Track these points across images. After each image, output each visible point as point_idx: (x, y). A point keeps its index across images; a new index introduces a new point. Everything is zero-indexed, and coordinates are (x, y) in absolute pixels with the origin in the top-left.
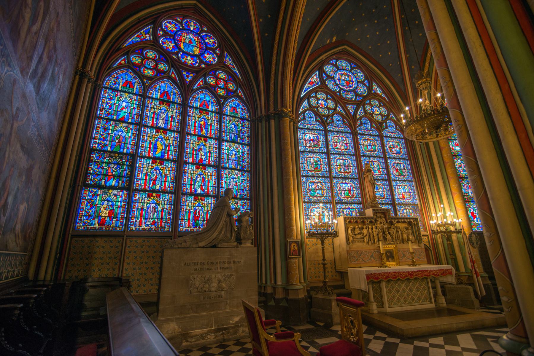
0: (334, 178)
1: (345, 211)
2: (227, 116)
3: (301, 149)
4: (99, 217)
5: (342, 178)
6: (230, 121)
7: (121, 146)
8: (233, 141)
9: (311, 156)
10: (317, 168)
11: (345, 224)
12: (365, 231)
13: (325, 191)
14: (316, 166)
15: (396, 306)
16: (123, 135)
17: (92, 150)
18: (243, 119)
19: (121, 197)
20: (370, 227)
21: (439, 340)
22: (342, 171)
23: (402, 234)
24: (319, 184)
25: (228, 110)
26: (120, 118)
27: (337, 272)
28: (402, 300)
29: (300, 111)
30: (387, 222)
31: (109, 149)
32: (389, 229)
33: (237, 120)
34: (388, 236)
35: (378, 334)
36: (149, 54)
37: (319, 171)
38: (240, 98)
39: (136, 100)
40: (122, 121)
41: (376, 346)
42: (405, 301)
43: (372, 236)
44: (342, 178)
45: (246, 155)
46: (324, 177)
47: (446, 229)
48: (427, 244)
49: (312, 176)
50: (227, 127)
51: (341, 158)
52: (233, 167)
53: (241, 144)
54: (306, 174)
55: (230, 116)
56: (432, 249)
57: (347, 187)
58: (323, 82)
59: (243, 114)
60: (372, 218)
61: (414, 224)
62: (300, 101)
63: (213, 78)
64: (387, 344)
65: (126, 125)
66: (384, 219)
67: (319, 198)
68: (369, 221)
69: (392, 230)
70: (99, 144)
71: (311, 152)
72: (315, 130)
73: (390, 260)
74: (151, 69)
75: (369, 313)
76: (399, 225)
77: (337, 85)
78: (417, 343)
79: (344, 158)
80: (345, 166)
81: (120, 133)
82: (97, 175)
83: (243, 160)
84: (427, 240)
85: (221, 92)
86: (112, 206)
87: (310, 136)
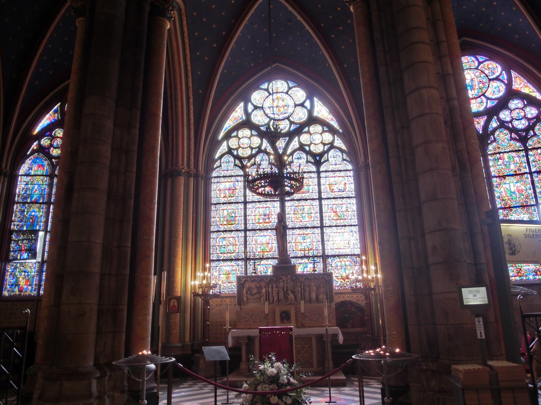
0: (250, 230)
1: (259, 267)
3: (214, 201)
4: (18, 285)
5: (260, 230)
7: (34, 225)
9: (225, 208)
12: (264, 290)
13: (237, 247)
16: (36, 215)
17: (12, 232)
19: (35, 268)
22: (261, 221)
24: (231, 239)
26: (33, 200)
29: (217, 156)
31: (25, 229)
34: (291, 296)
36: (57, 133)
37: (232, 224)
39: (46, 181)
40: (36, 202)
43: (270, 295)
44: (260, 230)
47: (366, 286)
49: (223, 231)
51: (261, 206)
54: (217, 229)
57: (264, 240)
58: (248, 115)
62: (219, 143)
65: (38, 205)
67: (229, 255)
70: (18, 225)
71: (226, 203)
72: (232, 176)
73: (285, 321)
74: (58, 148)
77: (267, 115)
79: (265, 206)
80: (265, 215)
81: (33, 214)
82: (16, 251)
86: (28, 276)
87: (225, 184)
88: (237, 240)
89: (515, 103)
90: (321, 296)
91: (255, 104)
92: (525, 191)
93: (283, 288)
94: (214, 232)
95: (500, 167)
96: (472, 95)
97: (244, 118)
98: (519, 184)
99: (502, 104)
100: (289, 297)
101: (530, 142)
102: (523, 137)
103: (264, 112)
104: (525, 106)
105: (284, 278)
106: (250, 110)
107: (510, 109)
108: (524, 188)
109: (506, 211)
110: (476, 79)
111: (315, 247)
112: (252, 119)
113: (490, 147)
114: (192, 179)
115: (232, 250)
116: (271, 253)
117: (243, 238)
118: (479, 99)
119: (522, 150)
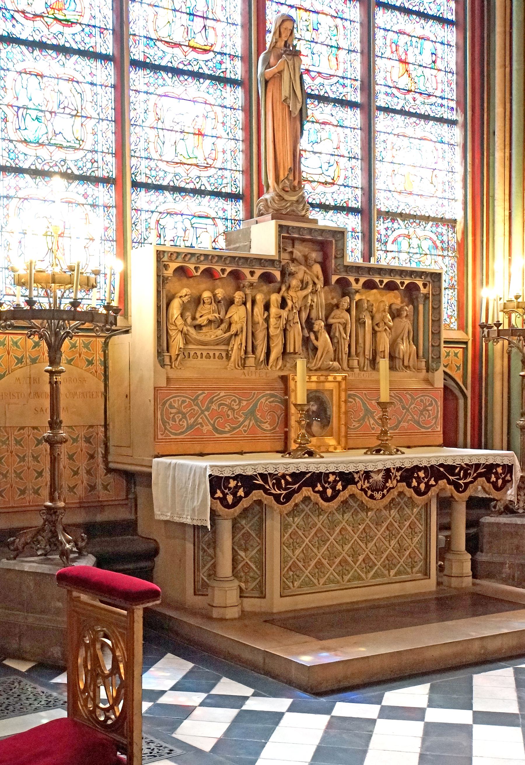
0: (136, 64)
11: (161, 281)
12: (238, 314)
13: (90, 124)
15: (305, 590)
20: (259, 297)
21: (415, 695)
23: (374, 333)
27: (109, 471)
28: (331, 571)
30: (327, 282)
32: (331, 308)
35: (227, 687)
41: (205, 727)
42: (342, 575)
43: (261, 335)
48: (458, 376)
56: (468, 393)
60: (271, 262)
61: (426, 297)
64: (244, 716)
66: (317, 268)
68: (258, 272)
69: (340, 317)
75: (209, 618)
76: (373, 295)
78: (343, 709)
84: (460, 362)
88: (88, 96)
90: (403, 347)
93: (299, 312)
100: (319, 344)
105: (300, 275)
111: (343, 174)
116: (211, 172)
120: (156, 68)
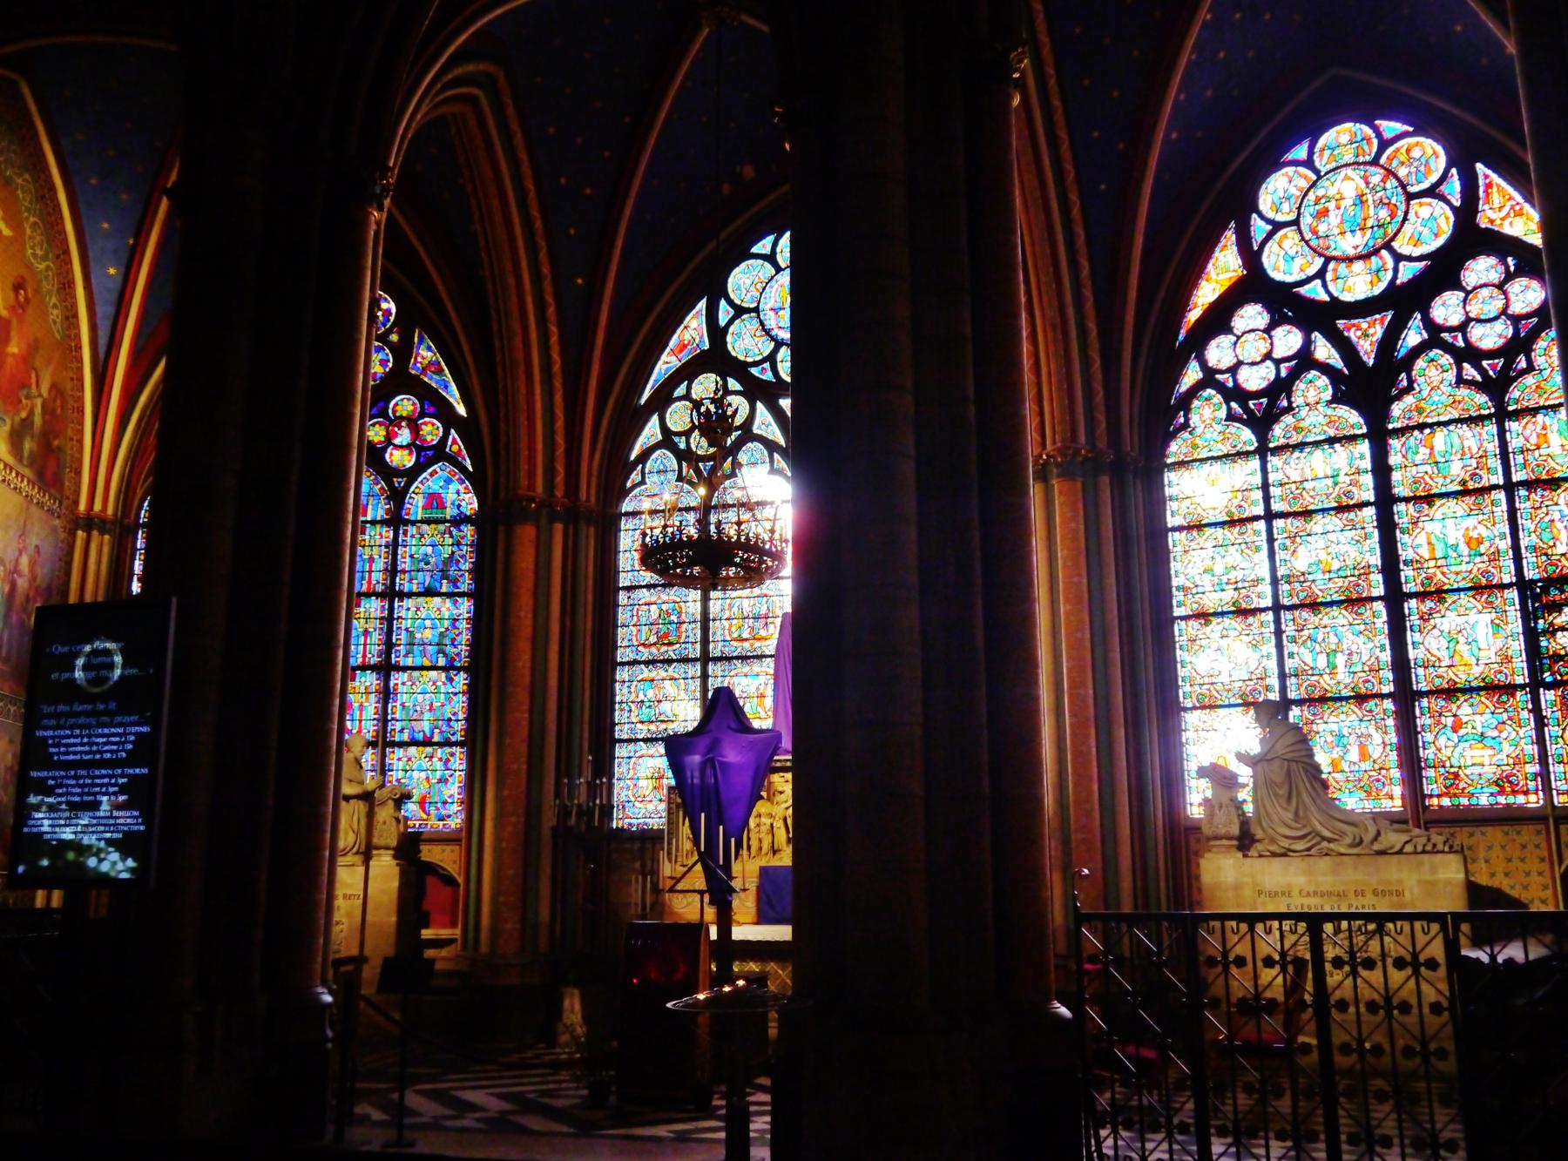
2: (413, 523)
5: (744, 658)
6: (422, 536)
8: (430, 592)
9: (653, 599)
10: (666, 635)
14: (664, 629)
18: (458, 521)
22: (745, 635)
25: (416, 506)
33: (442, 527)
37: (671, 644)
38: (453, 460)
44: (744, 658)
45: (463, 625)
46: (685, 660)
50: (412, 556)
52: (427, 663)
53: (449, 595)
54: (632, 657)
55: (422, 522)
58: (717, 334)
59: (459, 506)
63: (380, 424)
67: (663, 726)
77: (768, 332)
83: (453, 640)
85: (399, 458)
89: (1482, 269)
91: (738, 302)
92: (1487, 544)
94: (623, 664)
95: (1422, 468)
96: (1356, 248)
97: (707, 347)
98: (1472, 522)
99: (1443, 270)
101: (1515, 393)
102: (1497, 378)
103: (762, 324)
104: (1509, 277)
106: (723, 320)
107: (1462, 289)
108: (1485, 533)
109: (1429, 604)
110: (1370, 197)
112: (729, 347)
113: (1397, 409)
114: (559, 528)
115: (669, 713)
117: (698, 682)
118: (1373, 258)
119: (1489, 417)
120: (729, 659)
